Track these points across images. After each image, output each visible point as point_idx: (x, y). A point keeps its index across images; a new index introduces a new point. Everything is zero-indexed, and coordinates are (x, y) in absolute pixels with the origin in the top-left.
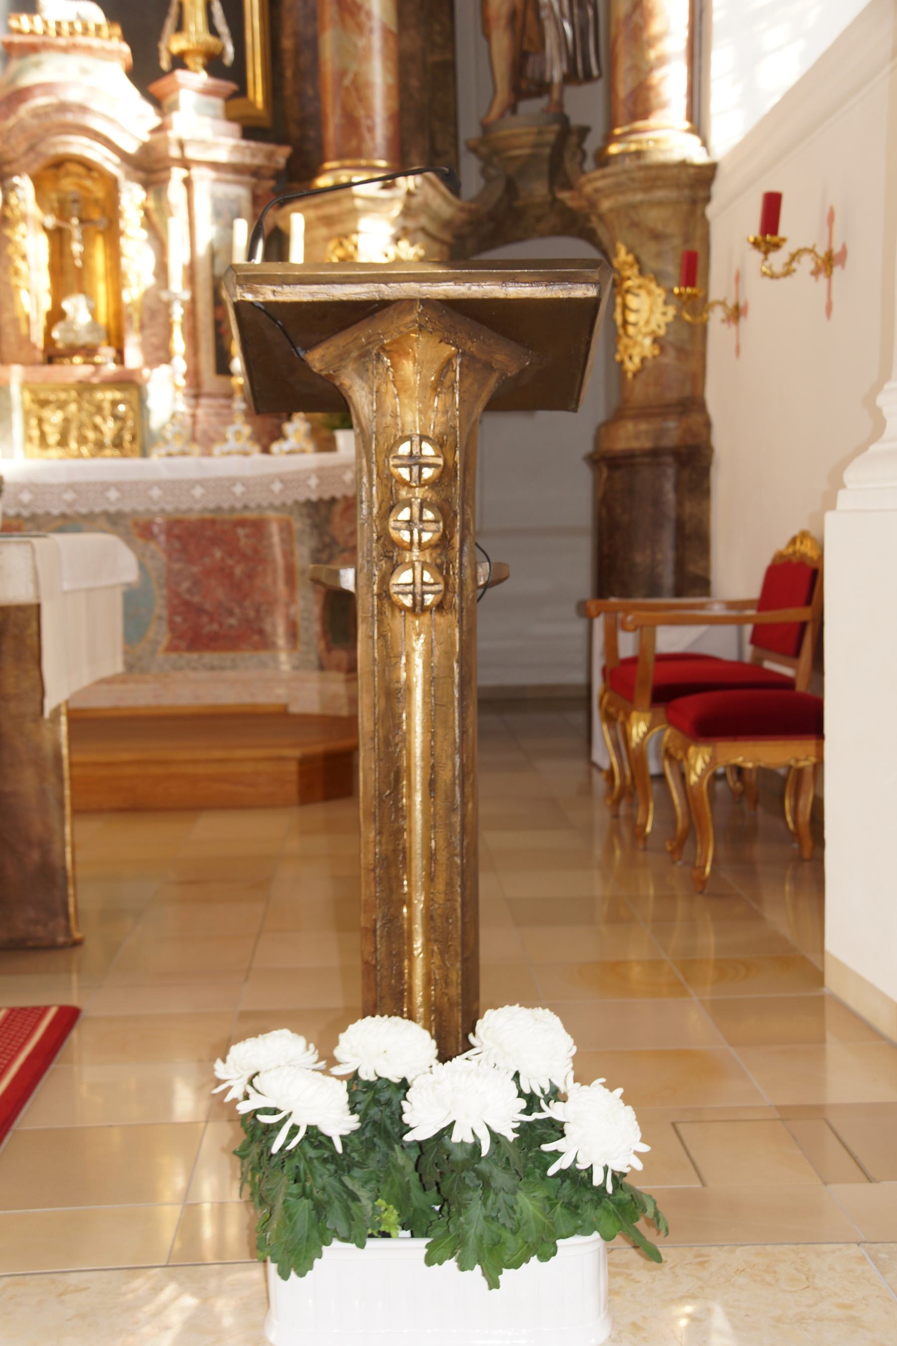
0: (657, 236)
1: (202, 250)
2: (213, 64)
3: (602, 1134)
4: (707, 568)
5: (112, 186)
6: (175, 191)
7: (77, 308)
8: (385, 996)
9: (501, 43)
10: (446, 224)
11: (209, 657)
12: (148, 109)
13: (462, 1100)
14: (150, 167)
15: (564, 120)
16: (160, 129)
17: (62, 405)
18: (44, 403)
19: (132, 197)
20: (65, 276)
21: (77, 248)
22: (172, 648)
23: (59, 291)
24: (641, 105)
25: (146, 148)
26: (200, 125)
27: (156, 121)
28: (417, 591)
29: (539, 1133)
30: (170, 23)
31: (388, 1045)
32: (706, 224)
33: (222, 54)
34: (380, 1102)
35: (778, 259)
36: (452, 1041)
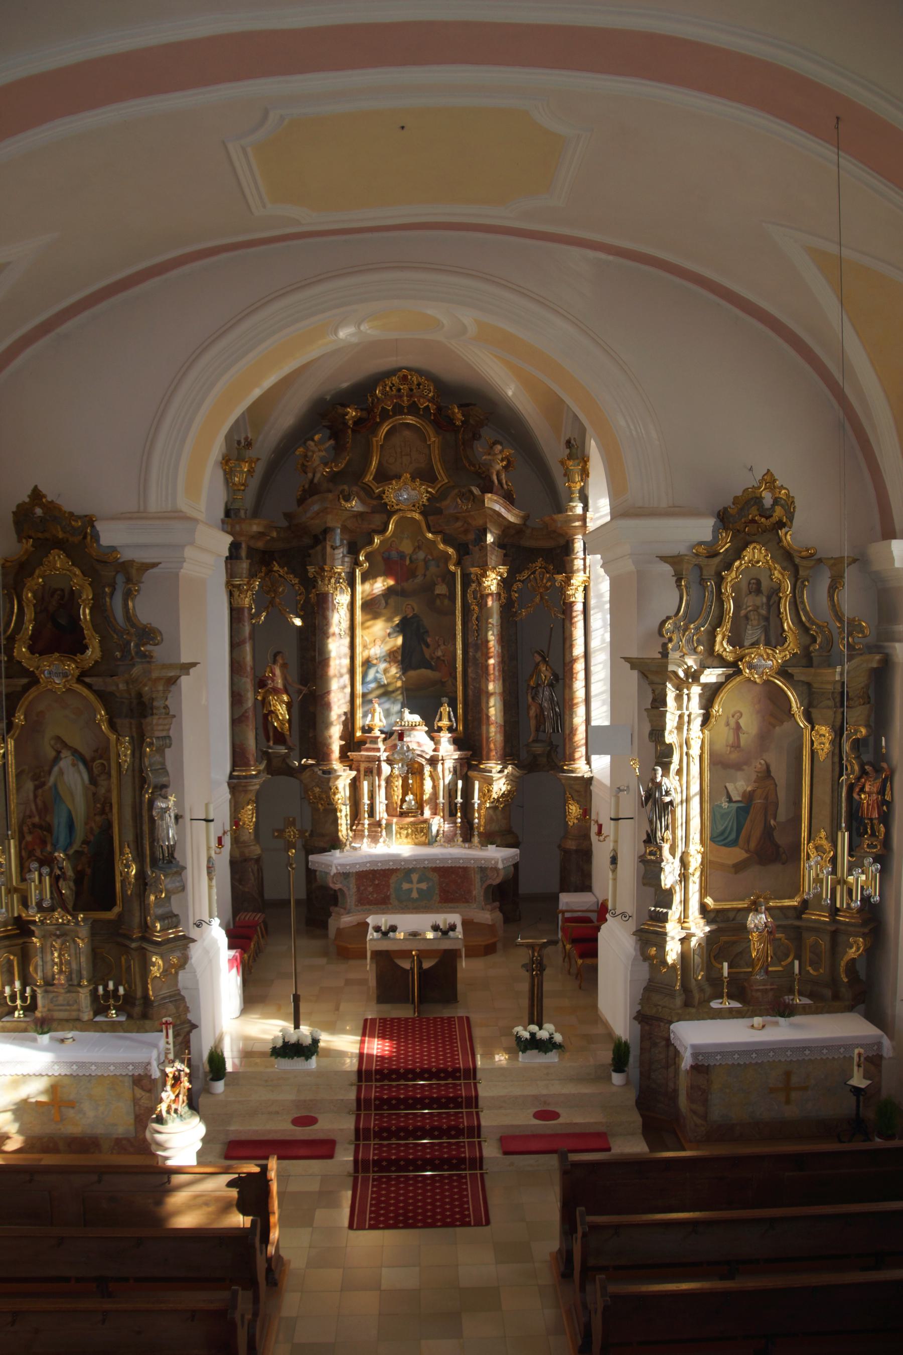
0: (578, 791)
1: (447, 782)
2: (450, 729)
3: (558, 1038)
4: (591, 883)
5: (422, 766)
6: (440, 767)
7: (409, 797)
8: (531, 1022)
9: (533, 723)
10: (517, 778)
11: (450, 905)
12: (432, 743)
13: (543, 1034)
14: (433, 761)
15: (551, 744)
16: (435, 750)
17: (407, 829)
18: (401, 828)
19: (427, 769)
20: (406, 789)
21: (410, 781)
22: (440, 902)
23: (405, 794)
24: (572, 759)
25: (432, 757)
26: (448, 752)
27: (433, 747)
28: (536, 974)
29: (551, 1038)
30: (438, 717)
31: (534, 1028)
32: (591, 791)
33: (452, 726)
34: (533, 1035)
35: (602, 838)
36: (541, 1028)
